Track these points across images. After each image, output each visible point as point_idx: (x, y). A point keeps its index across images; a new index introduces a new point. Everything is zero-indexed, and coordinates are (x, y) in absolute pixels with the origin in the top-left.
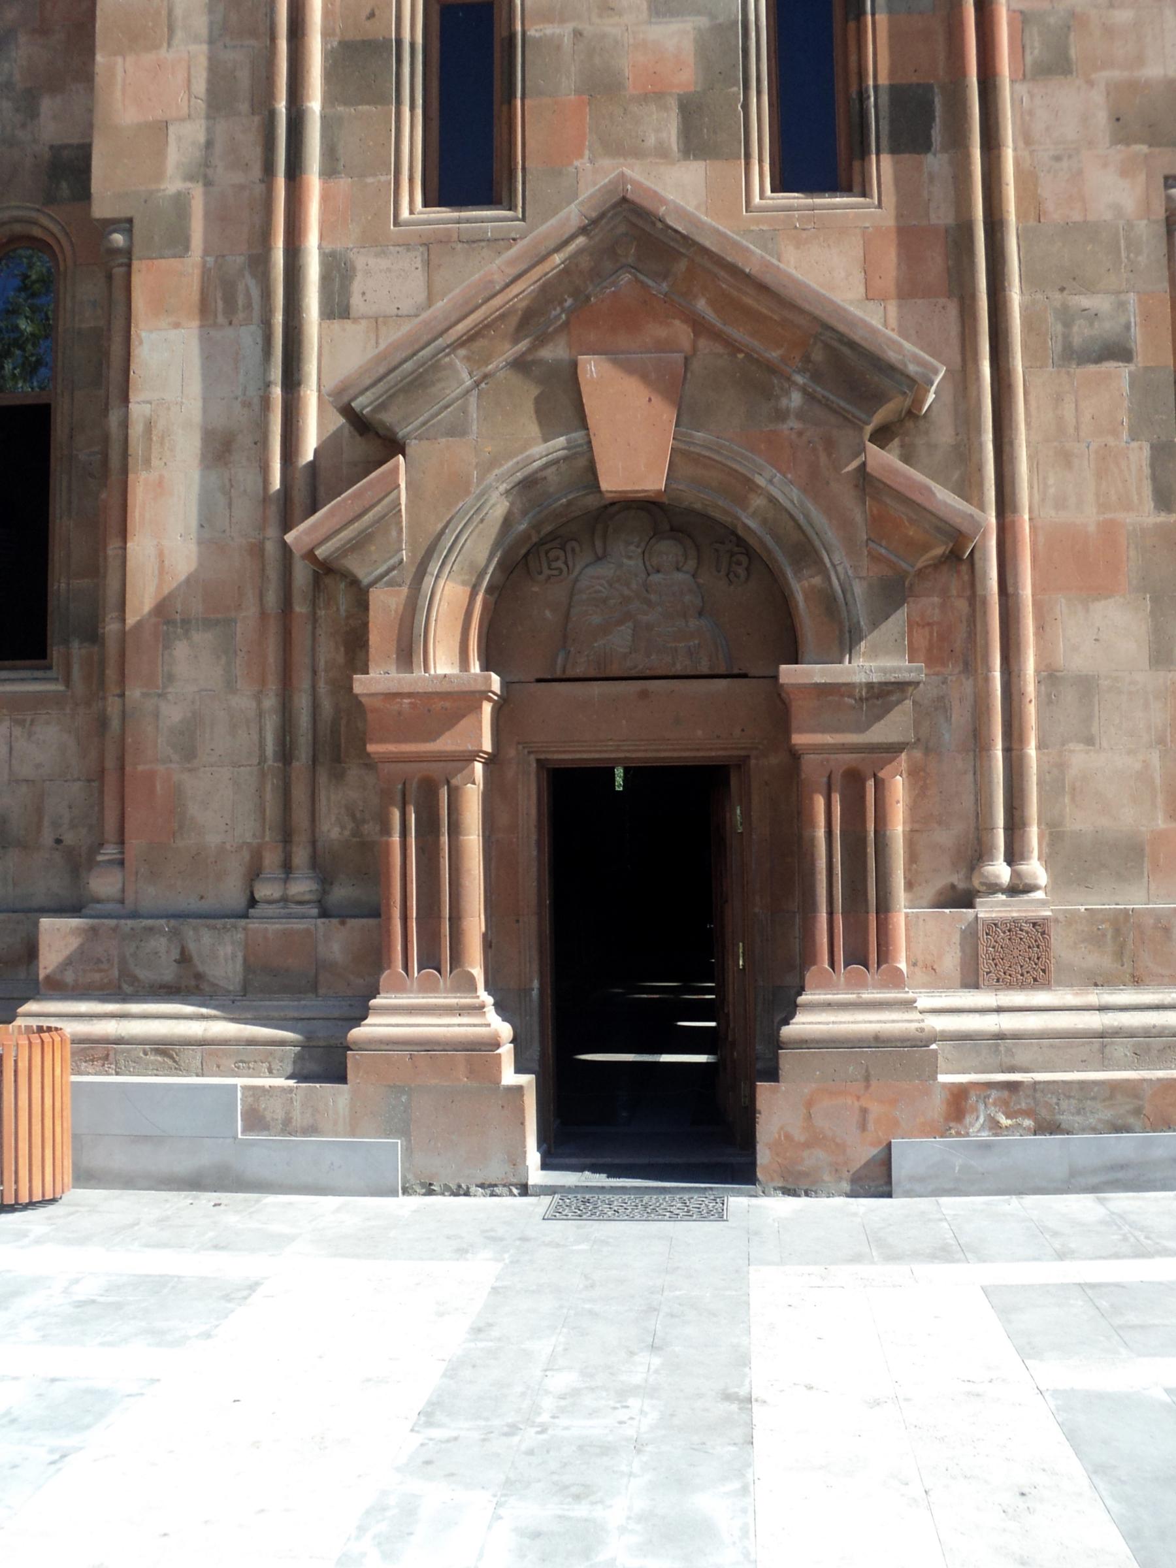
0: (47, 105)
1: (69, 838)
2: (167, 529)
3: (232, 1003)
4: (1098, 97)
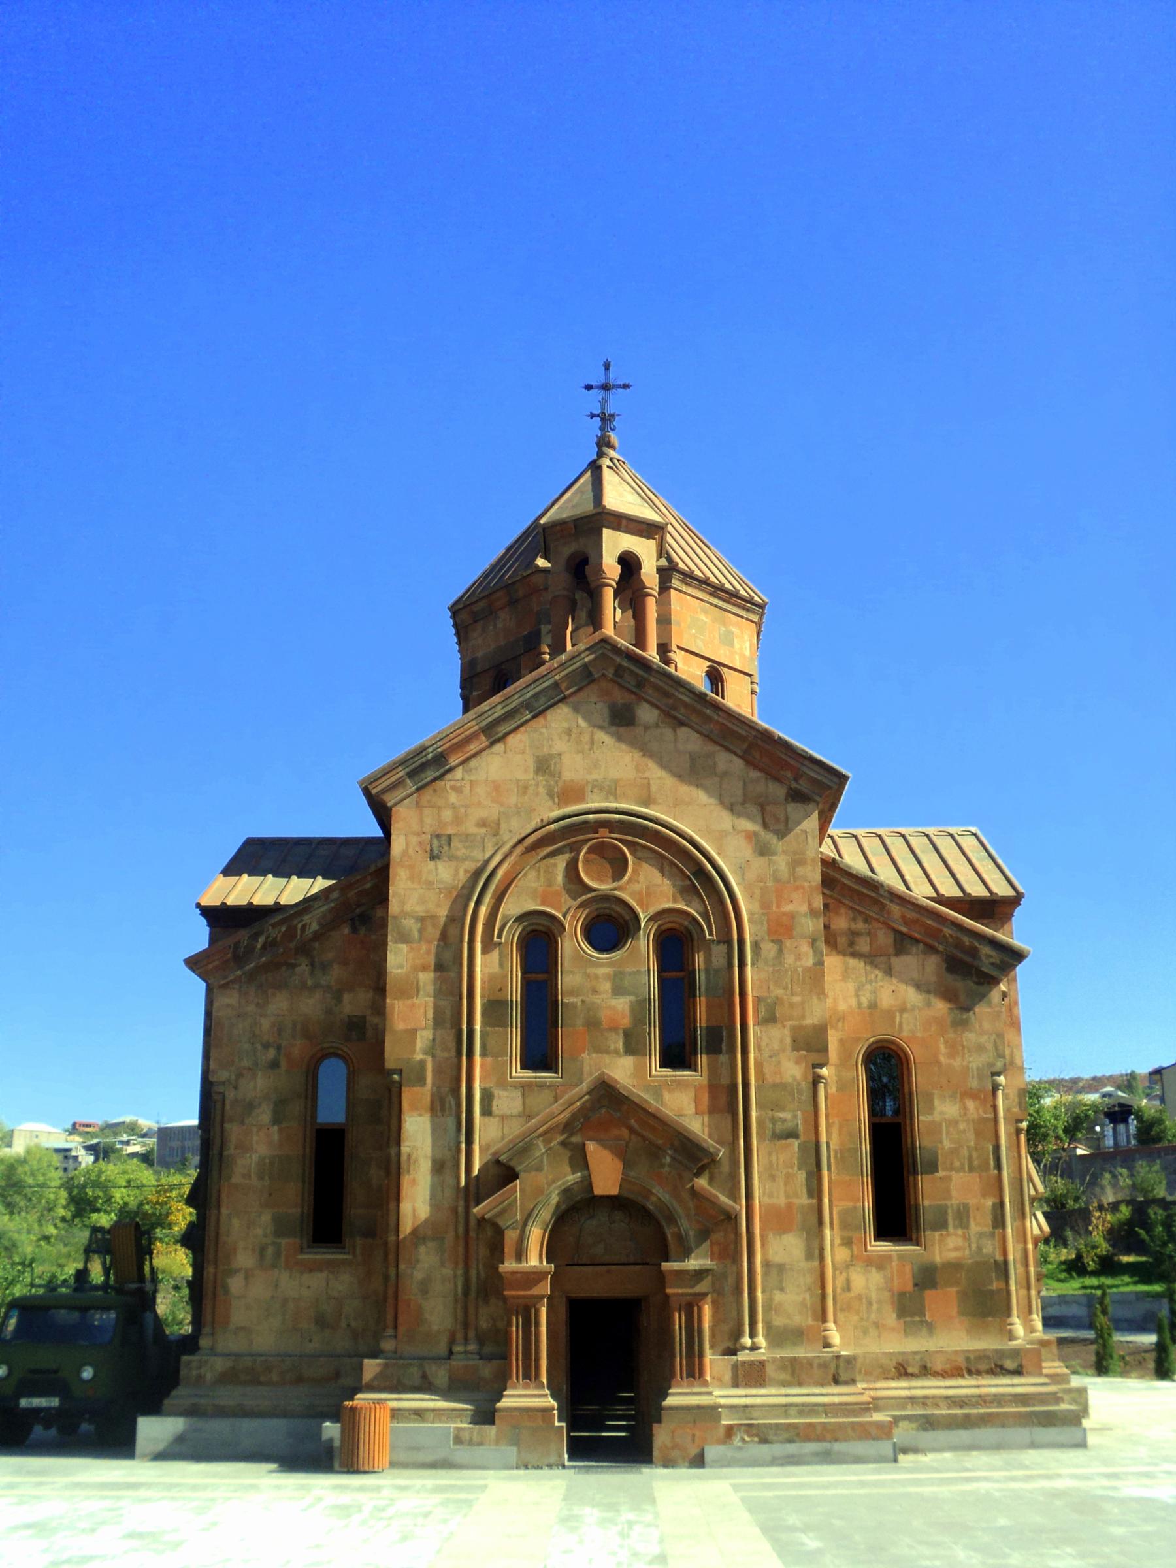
0: (347, 997)
1: (353, 1324)
2: (417, 1201)
3: (447, 1393)
4: (787, 1032)
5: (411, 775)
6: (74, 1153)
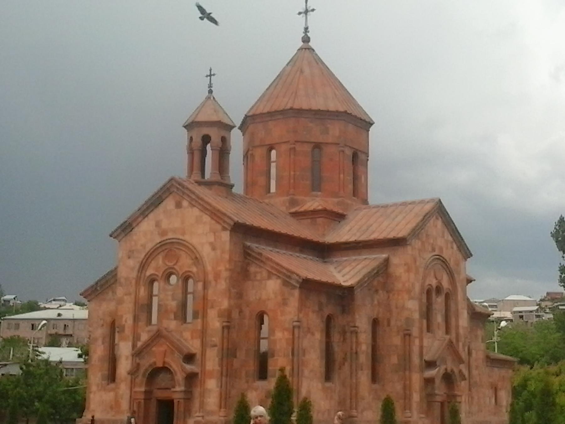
5: (123, 231)
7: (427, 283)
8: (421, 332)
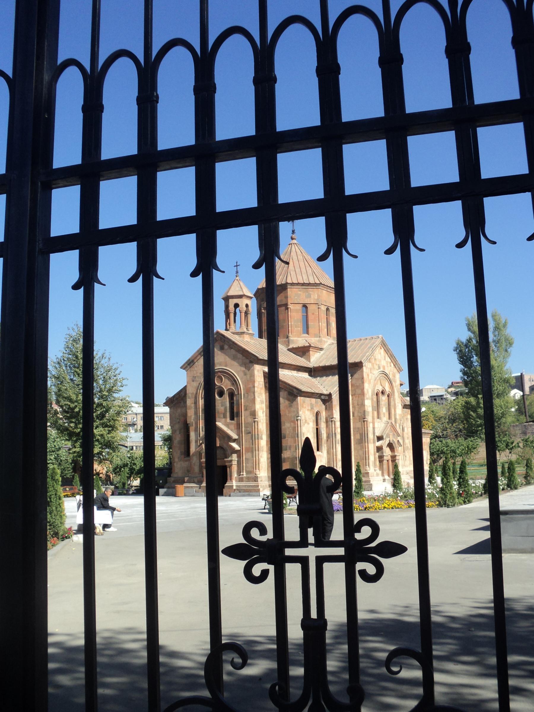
3: (197, 484)
5: (189, 365)
6: (445, 397)
7: (376, 388)
8: (373, 418)
